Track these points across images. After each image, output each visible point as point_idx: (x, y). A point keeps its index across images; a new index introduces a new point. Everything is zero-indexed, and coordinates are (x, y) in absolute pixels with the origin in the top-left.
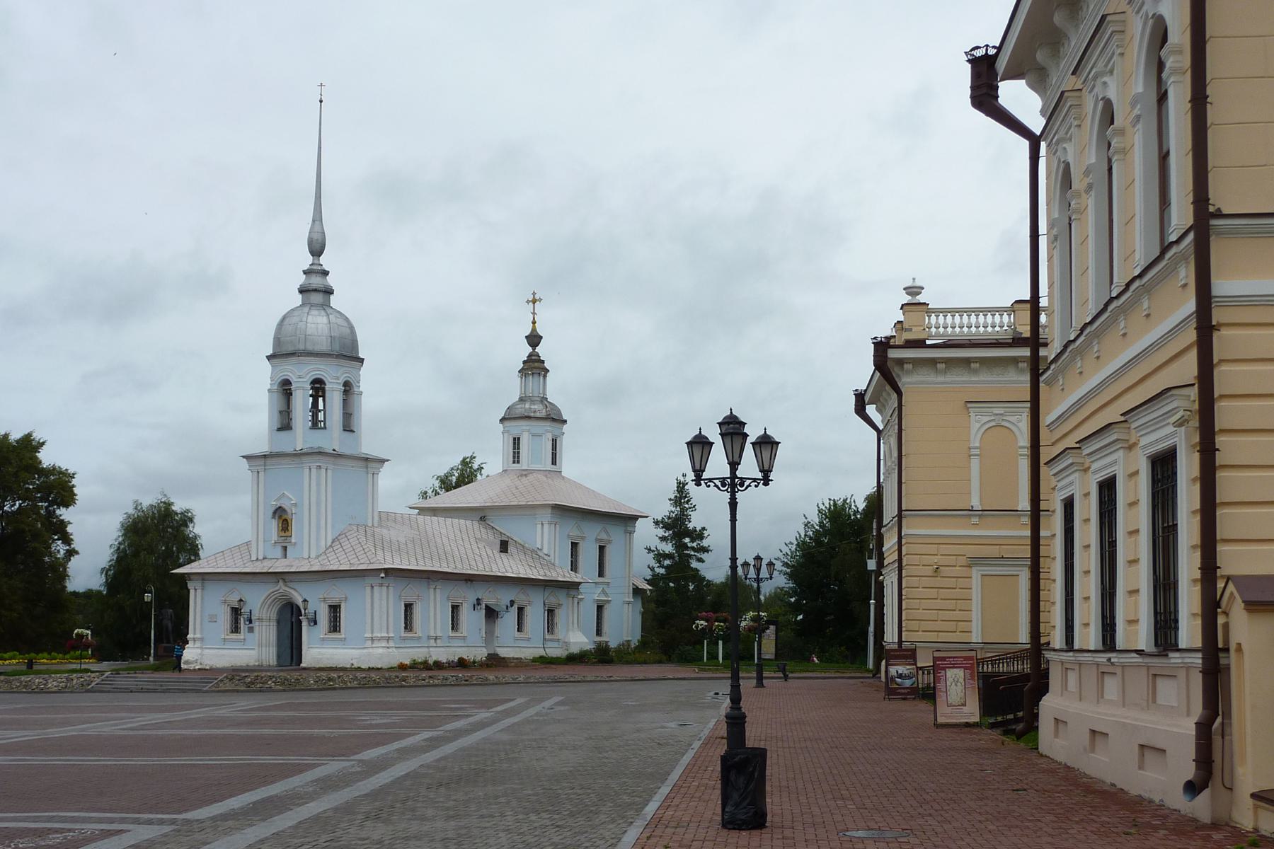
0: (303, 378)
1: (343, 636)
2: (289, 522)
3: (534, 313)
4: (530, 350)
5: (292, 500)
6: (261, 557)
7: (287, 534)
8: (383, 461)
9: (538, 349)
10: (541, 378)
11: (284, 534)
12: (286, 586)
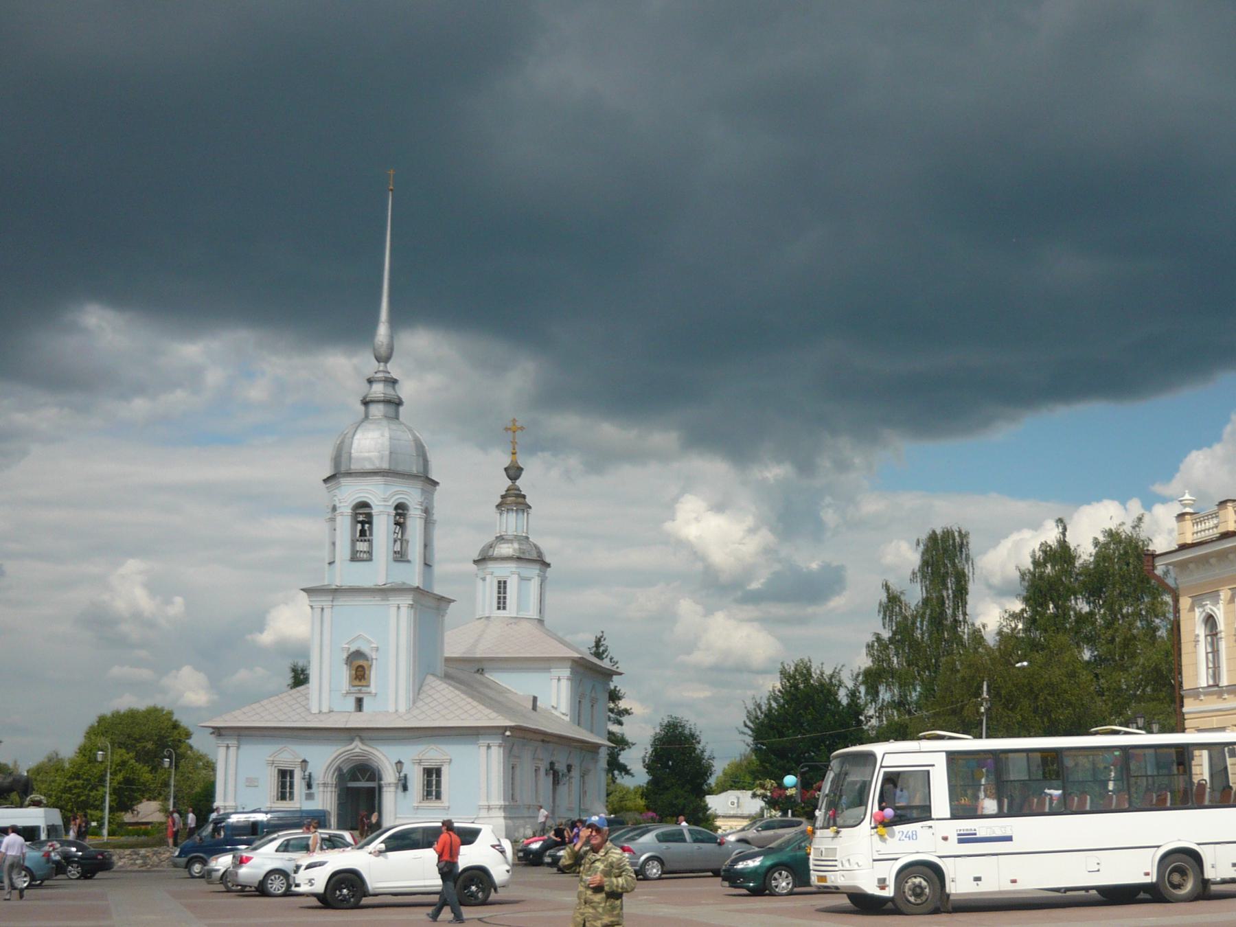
0: (387, 501)
1: (446, 804)
4: (509, 483)
5: (372, 643)
6: (325, 709)
7: (363, 683)
8: (450, 601)
9: (518, 483)
10: (525, 514)
11: (357, 683)
12: (363, 743)
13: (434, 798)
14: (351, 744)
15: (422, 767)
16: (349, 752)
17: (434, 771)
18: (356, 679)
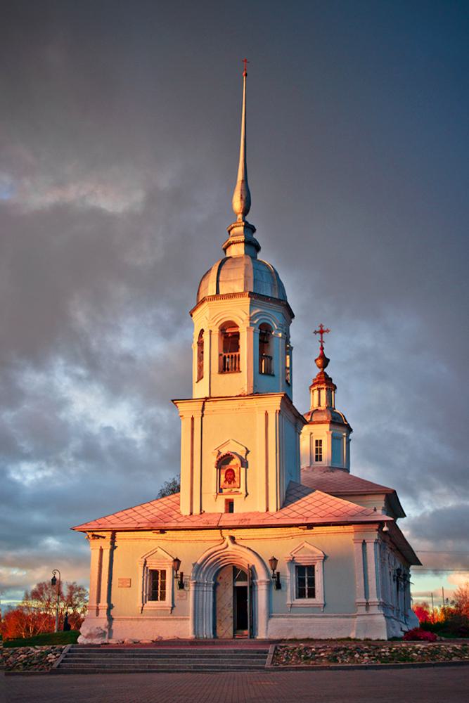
3: (322, 342)
4: (319, 371)
9: (325, 370)
13: (307, 596)
15: (294, 565)
17: (306, 570)
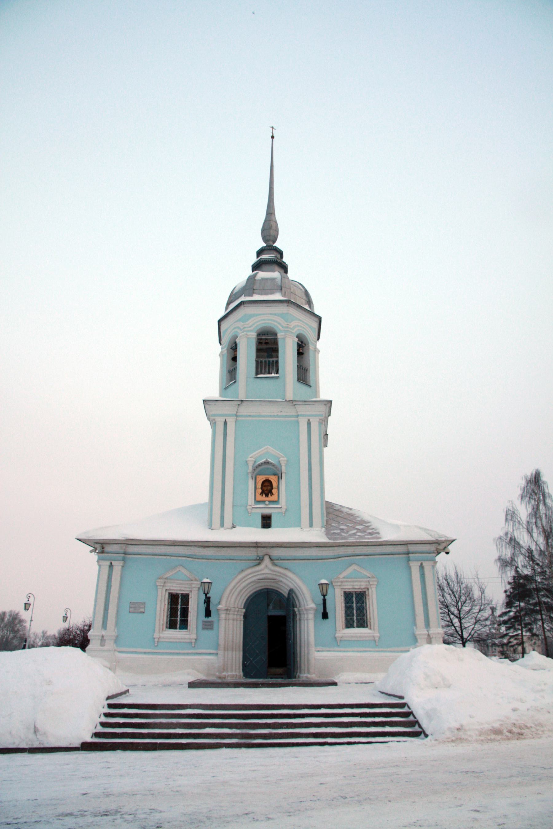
2: (275, 484)
7: (270, 498)
11: (264, 498)
14: (259, 564)
16: (257, 574)
18: (262, 494)
